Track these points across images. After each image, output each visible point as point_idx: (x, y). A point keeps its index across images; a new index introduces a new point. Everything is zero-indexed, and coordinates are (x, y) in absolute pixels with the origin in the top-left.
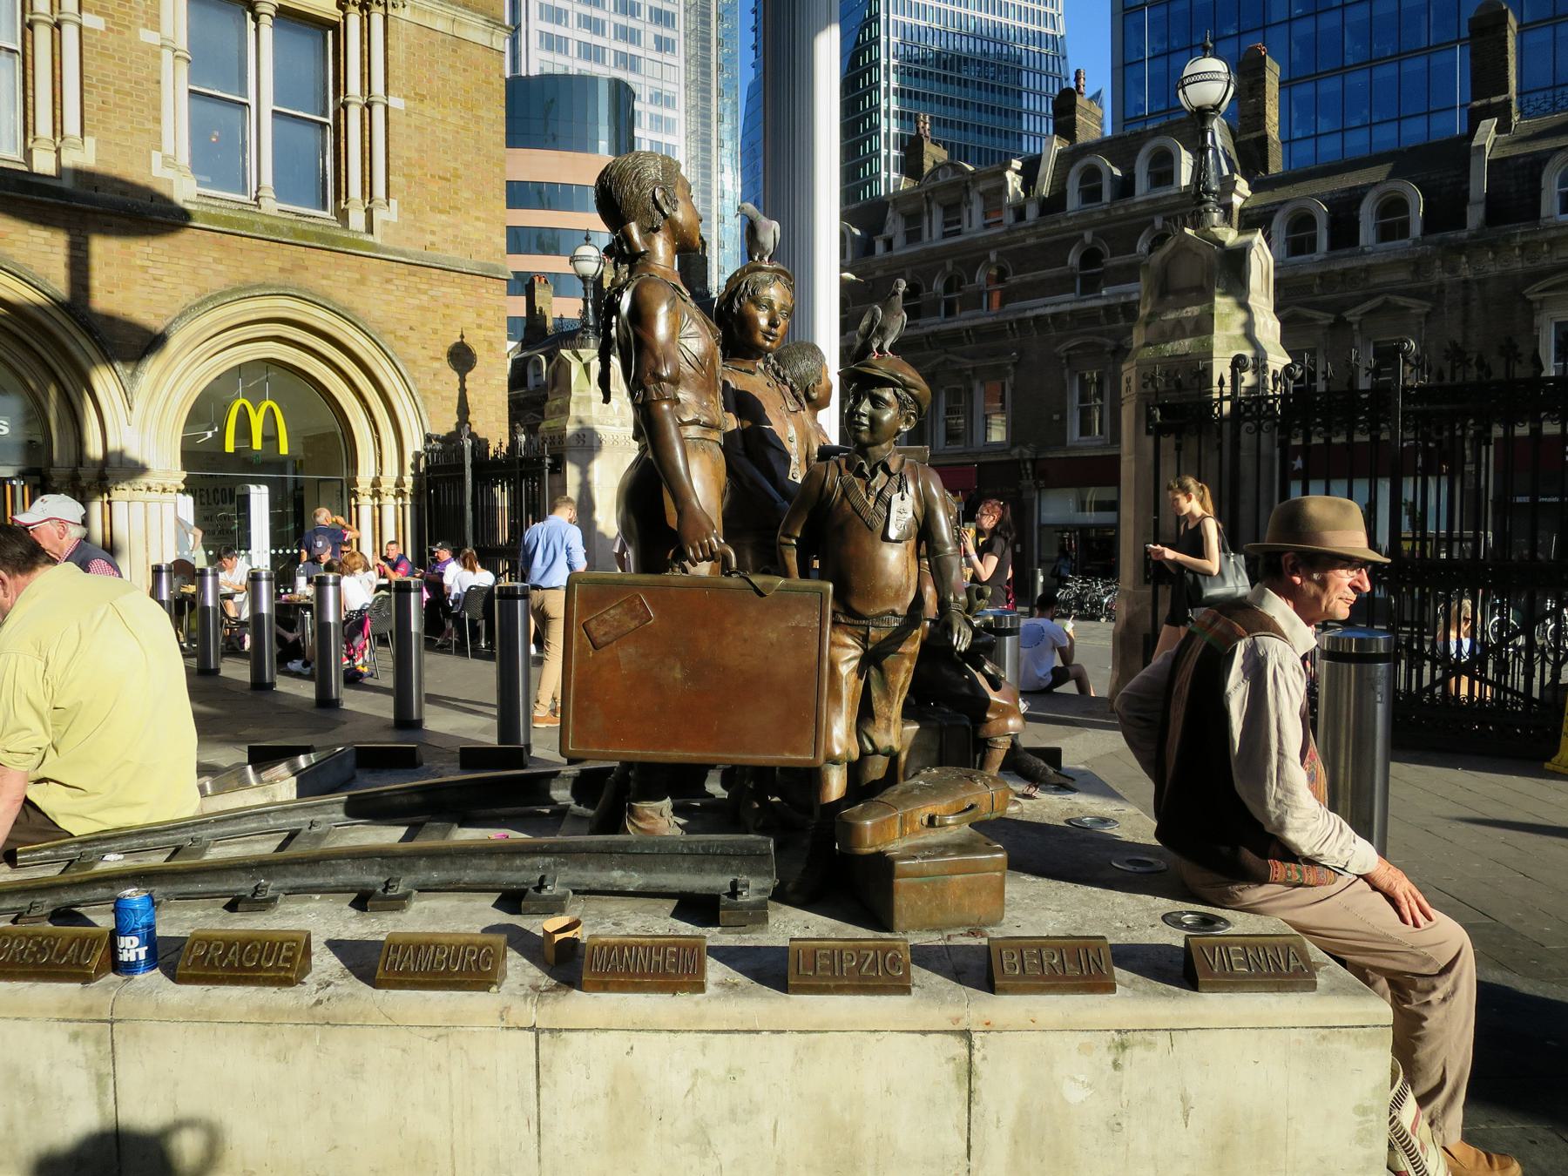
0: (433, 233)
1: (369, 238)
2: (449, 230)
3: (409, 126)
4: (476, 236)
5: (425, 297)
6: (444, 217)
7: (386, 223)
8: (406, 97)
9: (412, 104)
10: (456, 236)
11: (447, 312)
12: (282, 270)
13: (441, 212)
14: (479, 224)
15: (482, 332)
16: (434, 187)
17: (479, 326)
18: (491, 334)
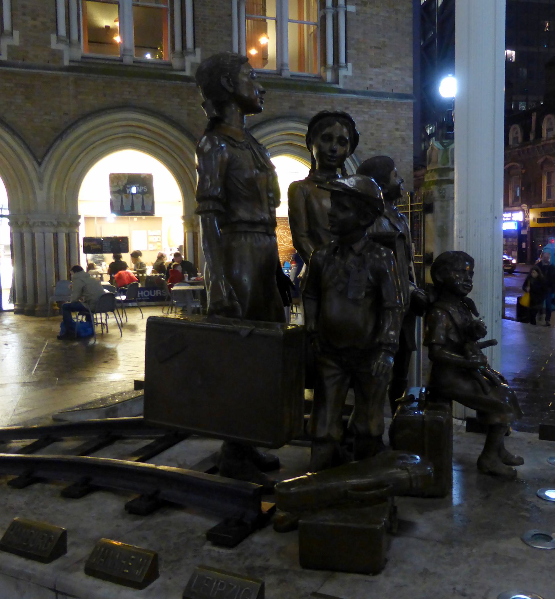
0: (371, 79)
1: (337, 86)
2: (380, 77)
3: (358, 20)
4: (394, 79)
5: (366, 117)
6: (377, 70)
7: (345, 77)
8: (356, 4)
9: (359, 8)
10: (384, 80)
11: (379, 123)
12: (291, 108)
13: (375, 67)
14: (398, 72)
15: (398, 133)
16: (372, 53)
17: (397, 130)
18: (404, 133)
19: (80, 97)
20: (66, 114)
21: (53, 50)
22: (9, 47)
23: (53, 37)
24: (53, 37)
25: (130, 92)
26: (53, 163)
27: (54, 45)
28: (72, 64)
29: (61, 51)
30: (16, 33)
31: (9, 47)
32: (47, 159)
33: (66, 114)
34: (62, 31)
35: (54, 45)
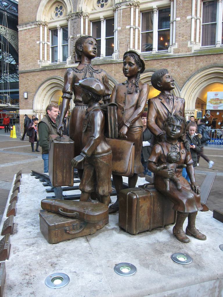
19: (197, 64)
20: (191, 71)
21: (189, 48)
22: (174, 49)
23: (189, 43)
24: (189, 43)
25: (217, 59)
26: (185, 90)
27: (189, 45)
28: (195, 51)
29: (191, 47)
30: (176, 44)
31: (174, 49)
32: (183, 88)
33: (191, 71)
34: (193, 39)
35: (189, 45)
